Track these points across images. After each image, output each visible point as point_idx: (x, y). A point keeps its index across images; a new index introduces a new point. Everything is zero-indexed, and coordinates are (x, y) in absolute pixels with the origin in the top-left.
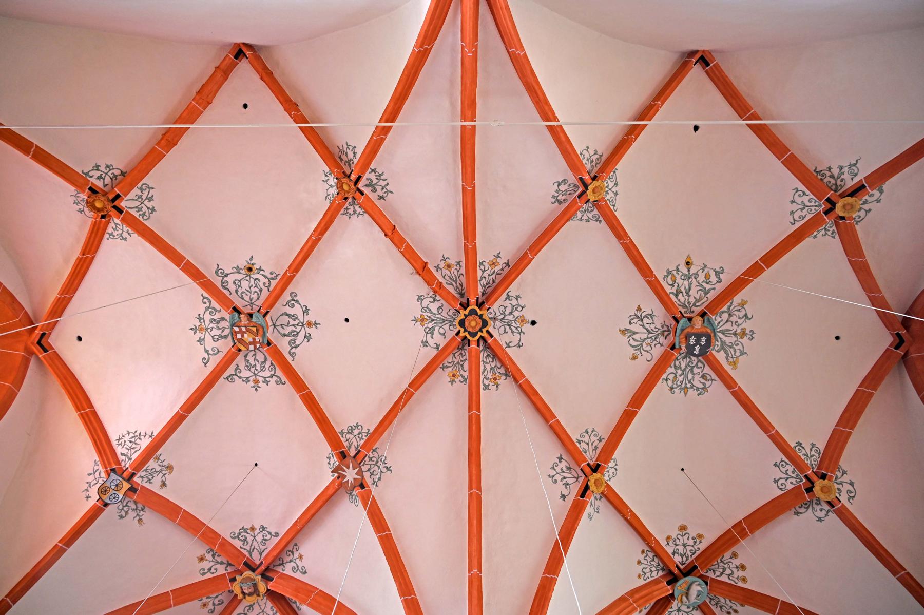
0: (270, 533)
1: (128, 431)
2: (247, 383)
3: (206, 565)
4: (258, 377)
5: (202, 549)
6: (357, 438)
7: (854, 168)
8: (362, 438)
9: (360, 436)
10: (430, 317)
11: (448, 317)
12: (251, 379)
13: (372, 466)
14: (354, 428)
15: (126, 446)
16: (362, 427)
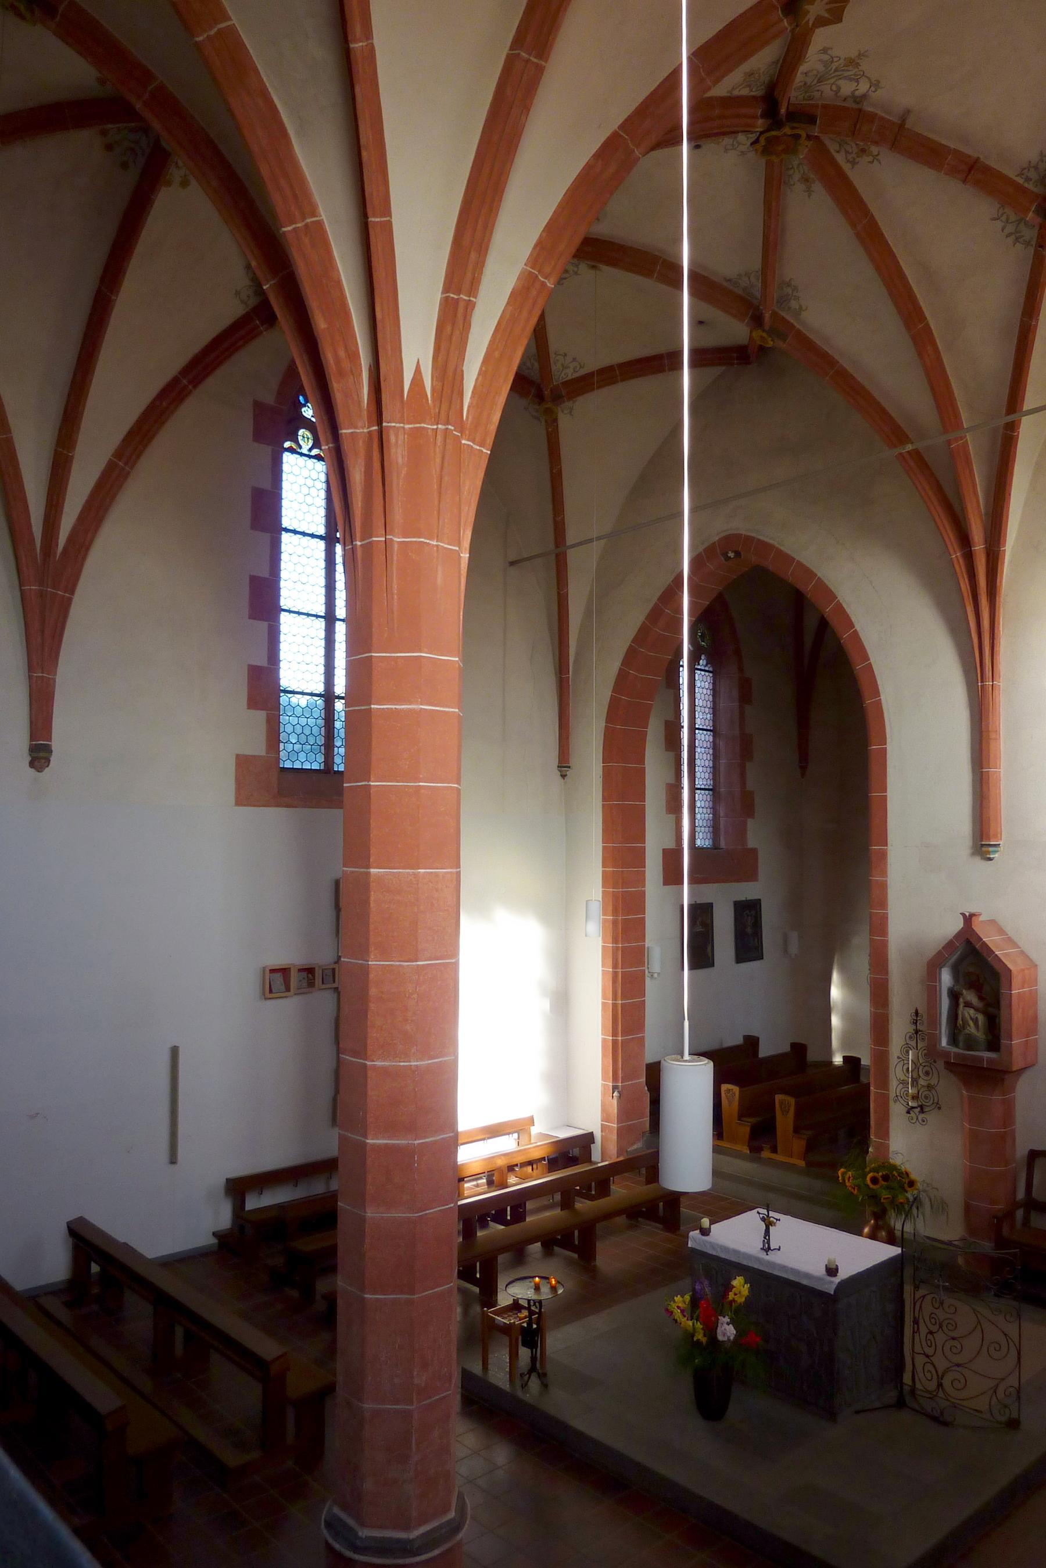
7: (569, 411)
10: (843, 70)
11: (818, 88)
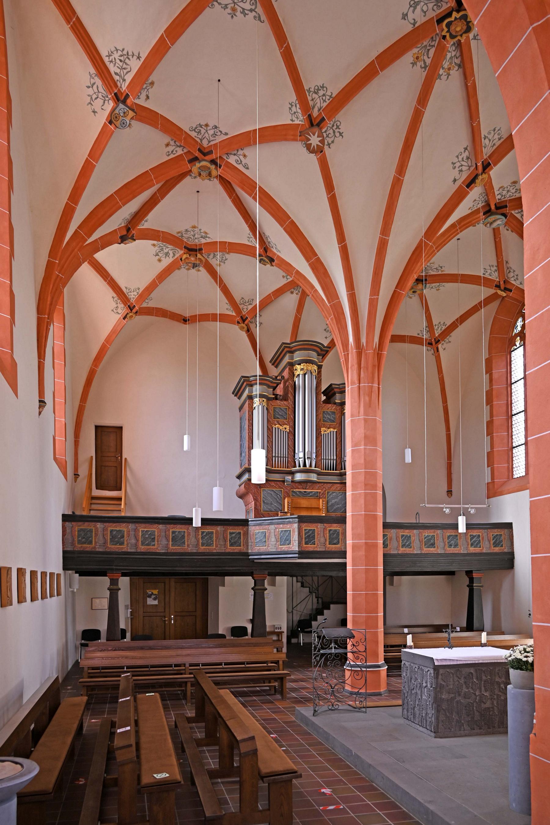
0: (221, 132)
1: (116, 48)
2: (225, 9)
3: (170, 149)
4: (236, 6)
5: (166, 139)
6: (321, 100)
8: (325, 101)
9: (324, 98)
12: (229, 6)
13: (329, 128)
14: (320, 88)
15: (117, 65)
16: (327, 89)
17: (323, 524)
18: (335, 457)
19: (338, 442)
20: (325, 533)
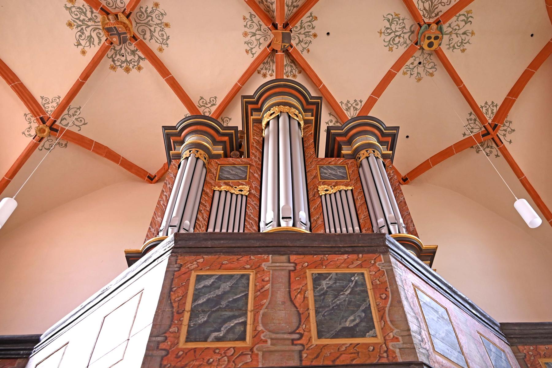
17: (284, 258)
18: (357, 228)
19: (358, 205)
20: (294, 287)
